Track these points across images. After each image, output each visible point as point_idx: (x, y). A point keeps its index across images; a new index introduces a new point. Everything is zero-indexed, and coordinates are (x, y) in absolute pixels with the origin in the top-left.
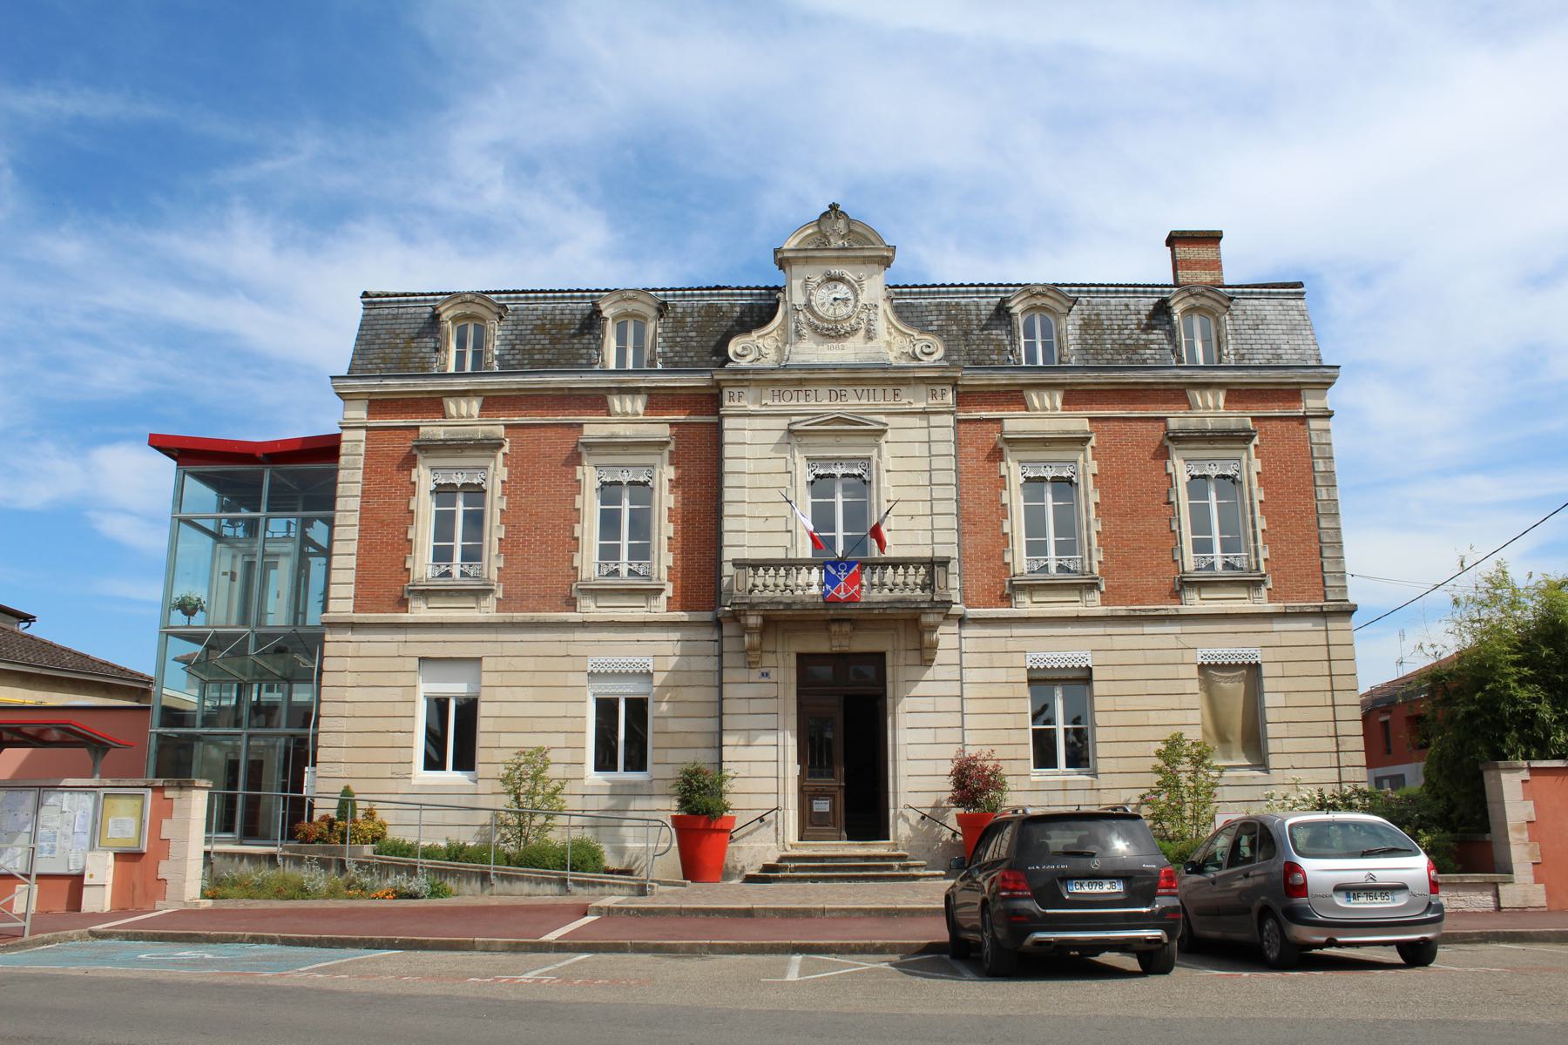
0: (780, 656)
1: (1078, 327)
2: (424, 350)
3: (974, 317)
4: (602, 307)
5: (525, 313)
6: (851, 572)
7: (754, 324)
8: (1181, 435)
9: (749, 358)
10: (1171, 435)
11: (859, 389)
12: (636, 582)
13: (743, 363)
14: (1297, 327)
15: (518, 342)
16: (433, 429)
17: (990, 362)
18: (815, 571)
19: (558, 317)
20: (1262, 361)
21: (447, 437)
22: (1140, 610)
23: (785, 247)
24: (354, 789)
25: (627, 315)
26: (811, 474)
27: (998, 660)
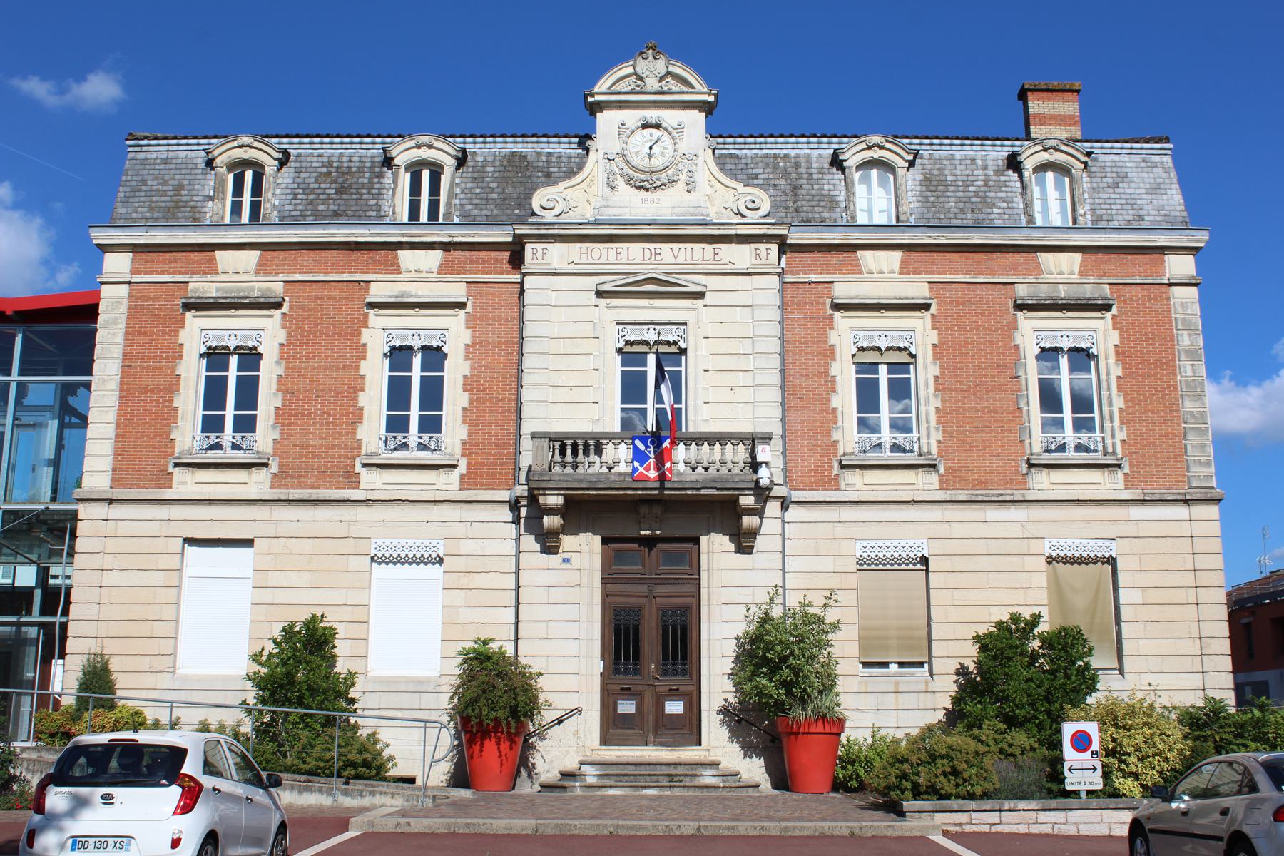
1: (918, 183)
2: (195, 198)
4: (394, 153)
5: (309, 159)
7: (561, 174)
10: (1019, 302)
13: (549, 217)
15: (301, 191)
19: (345, 165)
20: (1122, 223)
21: (218, 295)
22: (982, 495)
26: (621, 341)
27: (824, 547)
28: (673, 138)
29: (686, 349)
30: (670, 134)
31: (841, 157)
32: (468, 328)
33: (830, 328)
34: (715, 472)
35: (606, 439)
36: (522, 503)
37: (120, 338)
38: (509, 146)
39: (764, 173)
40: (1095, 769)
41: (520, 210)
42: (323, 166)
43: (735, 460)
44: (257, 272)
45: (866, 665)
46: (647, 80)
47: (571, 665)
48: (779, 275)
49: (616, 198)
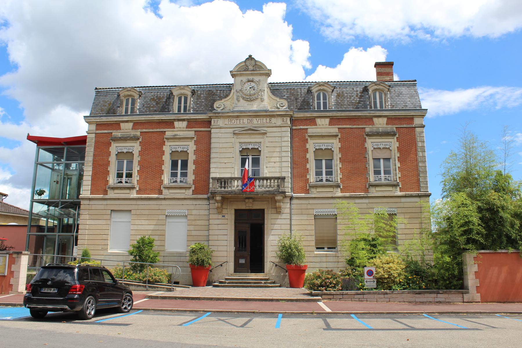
0: (229, 210)
1: (335, 96)
2: (114, 107)
3: (299, 94)
4: (173, 92)
6: (251, 182)
8: (370, 134)
10: (367, 134)
11: (258, 119)
12: (182, 185)
13: (219, 110)
14: (413, 96)
15: (145, 104)
16: (117, 133)
19: (159, 95)
22: (354, 195)
24: (91, 252)
25: (182, 94)
29: (260, 151)
32: (195, 145)
37: (92, 150)
40: (374, 281)
42: (152, 96)
44: (132, 129)
45: (317, 248)
47: (224, 249)
49: (239, 104)
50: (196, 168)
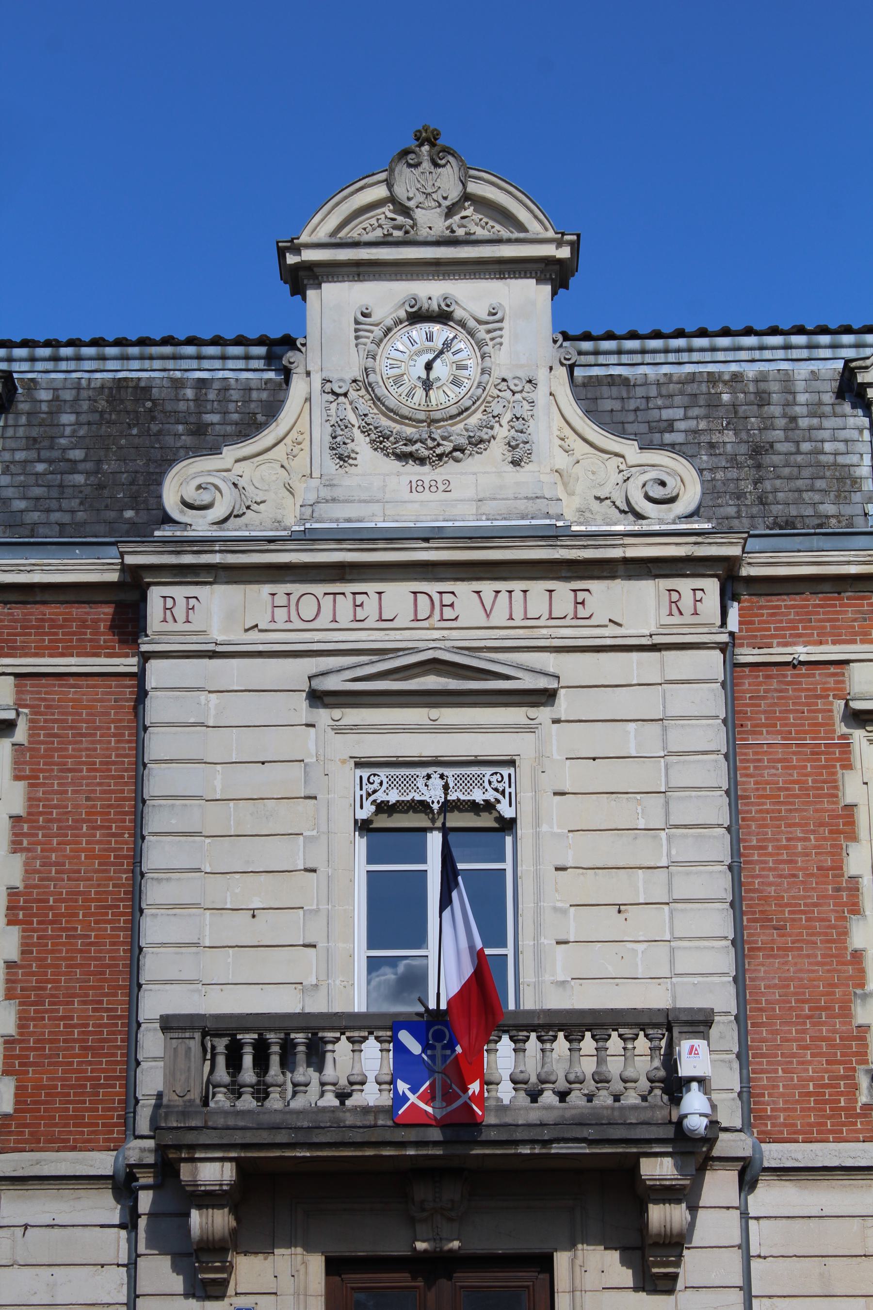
7: (229, 429)
9: (219, 511)
17: (817, 521)
18: (371, 1047)
23: (304, 238)
26: (367, 804)
28: (480, 344)
29: (513, 821)
30: (471, 333)
31: (861, 378)
32: (17, 778)
33: (844, 767)
34: (583, 1102)
35: (332, 1029)
36: (142, 1181)
38: (111, 365)
39: (686, 418)
41: (137, 511)
43: (630, 1073)
46: (419, 214)
48: (723, 648)
50: (25, 951)
